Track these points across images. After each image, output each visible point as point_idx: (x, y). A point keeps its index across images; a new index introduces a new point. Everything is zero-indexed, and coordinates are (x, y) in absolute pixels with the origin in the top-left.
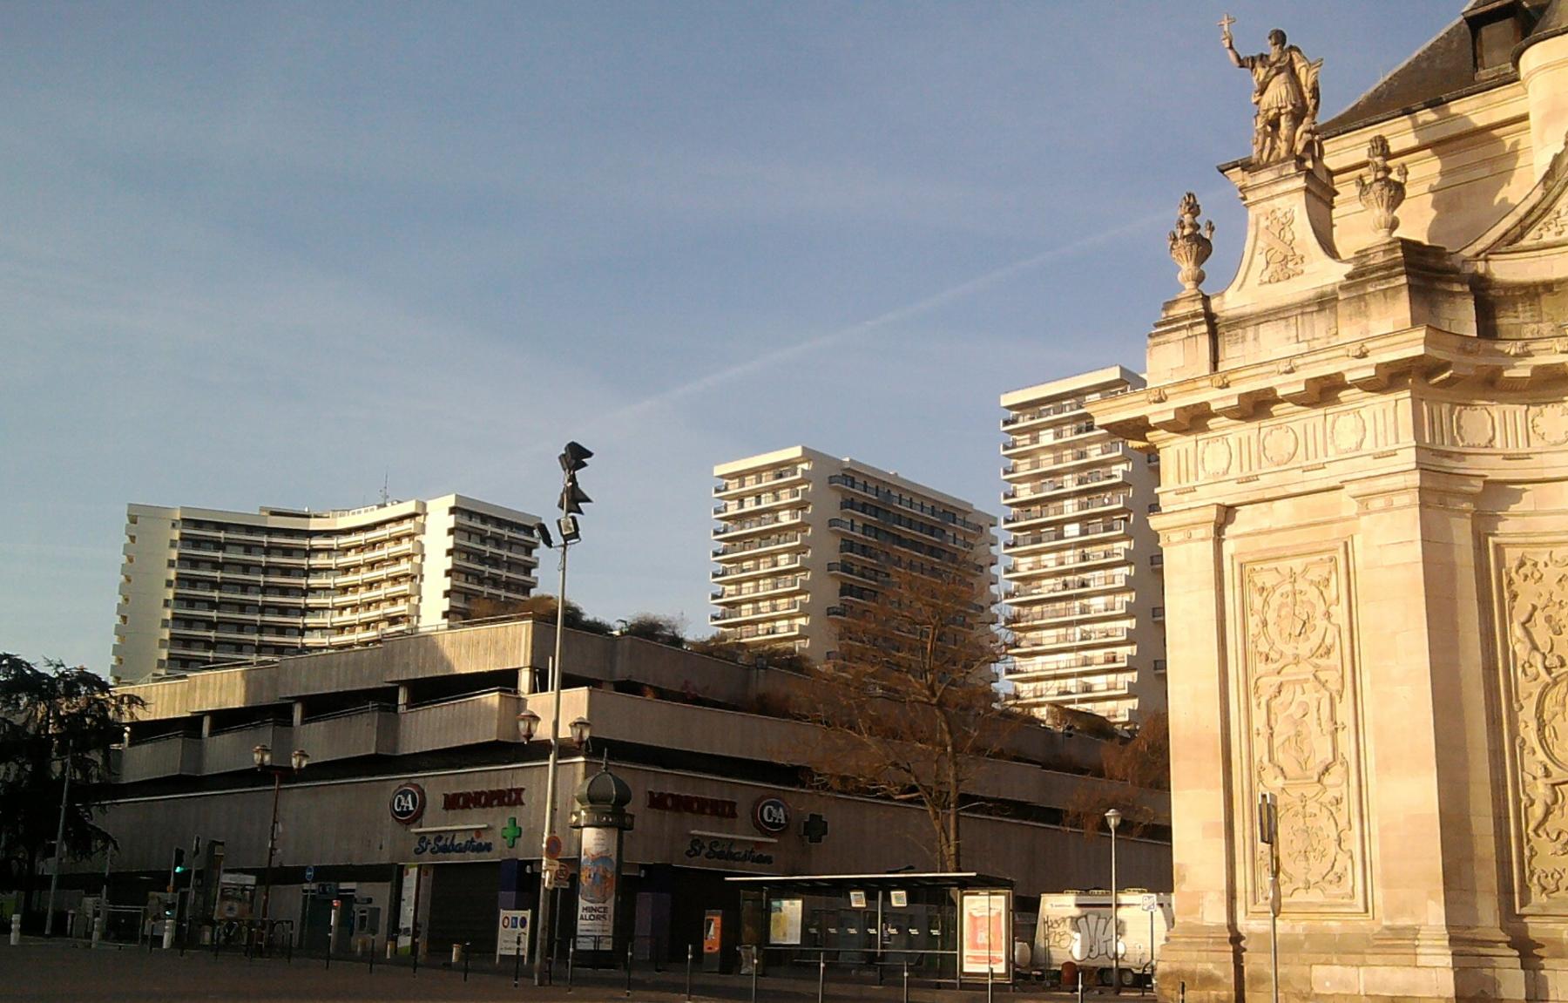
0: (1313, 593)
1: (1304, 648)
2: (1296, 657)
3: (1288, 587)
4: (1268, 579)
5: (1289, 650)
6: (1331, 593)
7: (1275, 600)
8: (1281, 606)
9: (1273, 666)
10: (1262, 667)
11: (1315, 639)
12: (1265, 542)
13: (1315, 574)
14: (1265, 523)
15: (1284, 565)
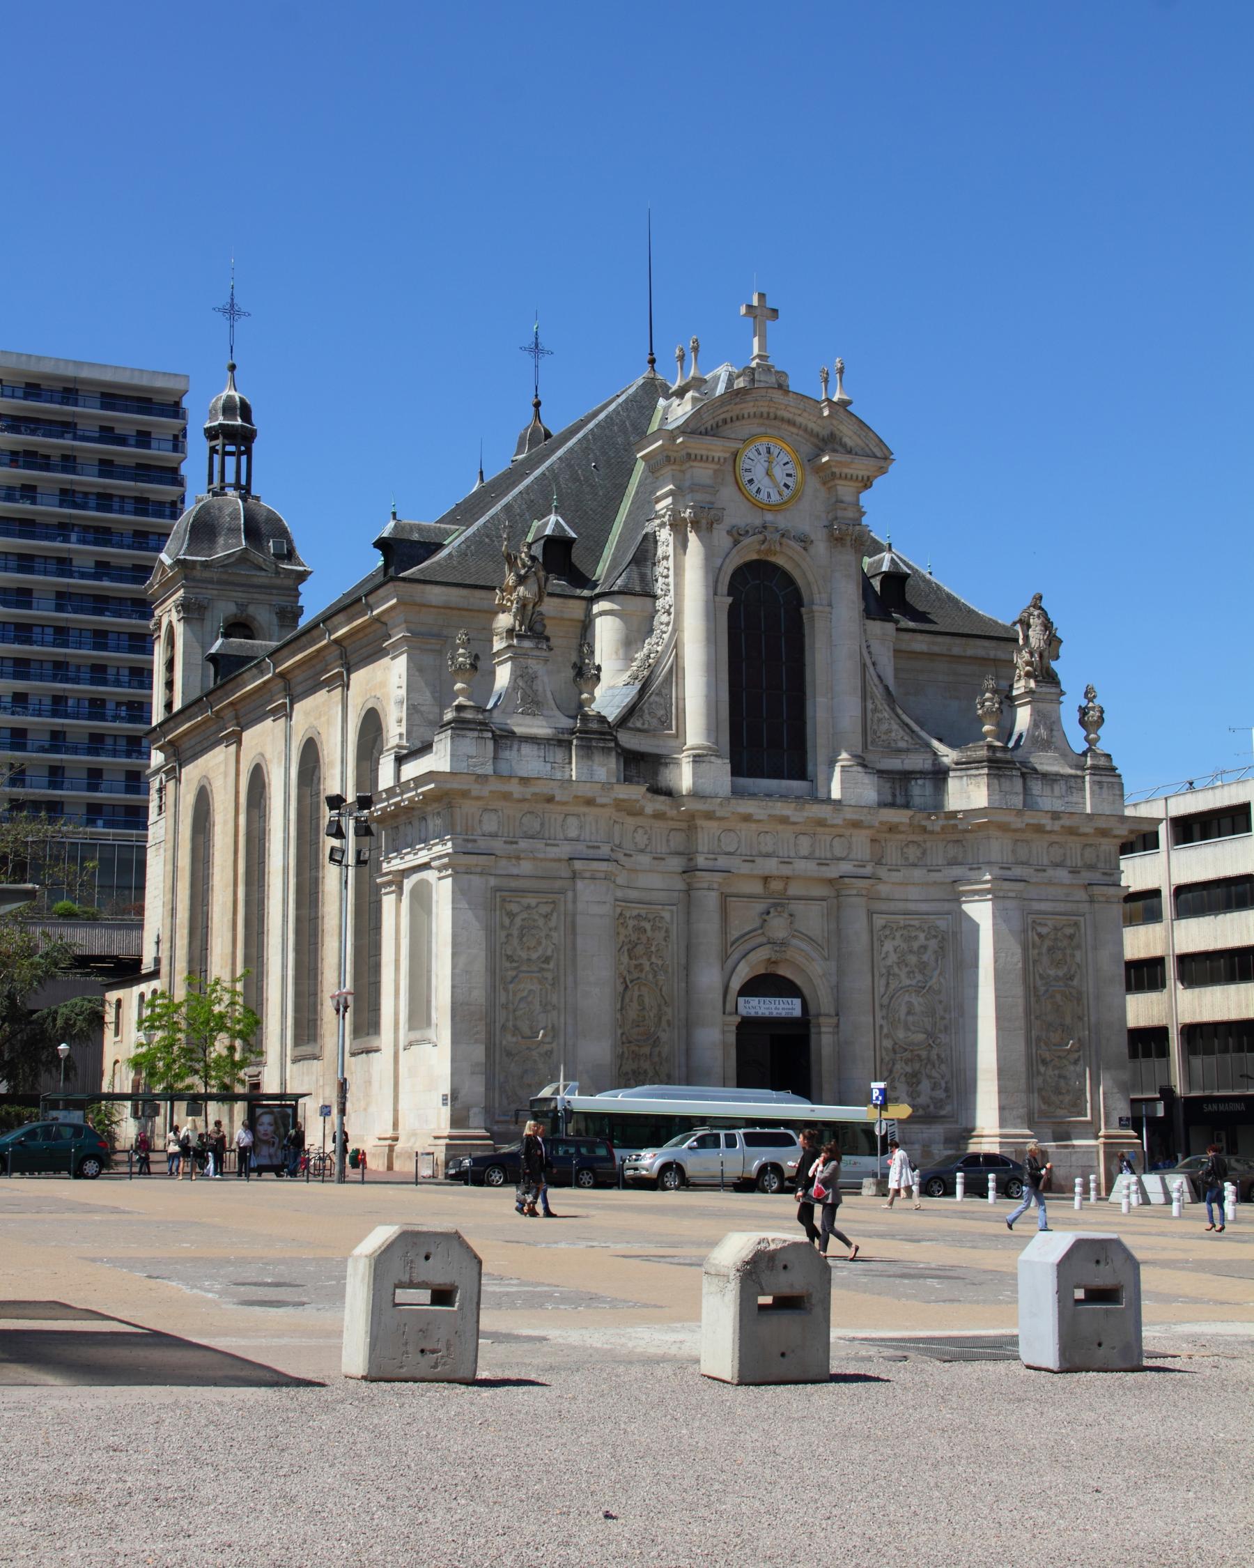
0: (541, 922)
1: (534, 956)
2: (529, 960)
3: (524, 915)
4: (514, 908)
5: (524, 955)
6: (553, 924)
7: (518, 921)
8: (522, 928)
9: (515, 965)
10: (508, 965)
11: (540, 951)
12: (514, 884)
13: (544, 909)
14: (515, 871)
15: (525, 901)
